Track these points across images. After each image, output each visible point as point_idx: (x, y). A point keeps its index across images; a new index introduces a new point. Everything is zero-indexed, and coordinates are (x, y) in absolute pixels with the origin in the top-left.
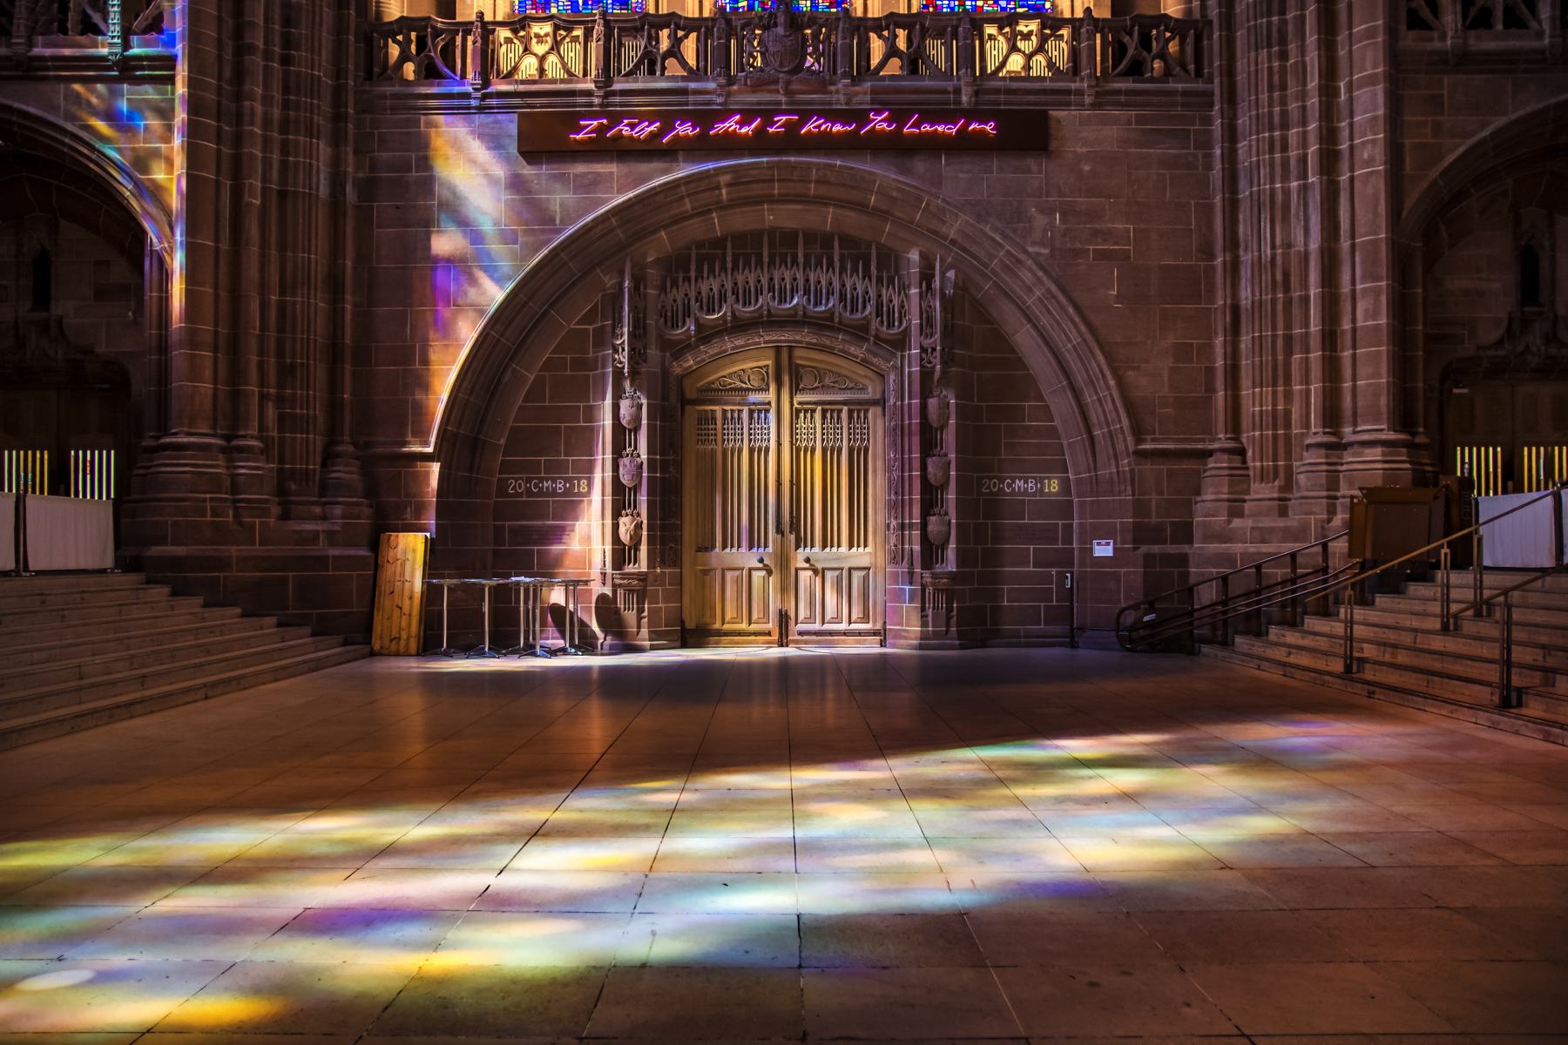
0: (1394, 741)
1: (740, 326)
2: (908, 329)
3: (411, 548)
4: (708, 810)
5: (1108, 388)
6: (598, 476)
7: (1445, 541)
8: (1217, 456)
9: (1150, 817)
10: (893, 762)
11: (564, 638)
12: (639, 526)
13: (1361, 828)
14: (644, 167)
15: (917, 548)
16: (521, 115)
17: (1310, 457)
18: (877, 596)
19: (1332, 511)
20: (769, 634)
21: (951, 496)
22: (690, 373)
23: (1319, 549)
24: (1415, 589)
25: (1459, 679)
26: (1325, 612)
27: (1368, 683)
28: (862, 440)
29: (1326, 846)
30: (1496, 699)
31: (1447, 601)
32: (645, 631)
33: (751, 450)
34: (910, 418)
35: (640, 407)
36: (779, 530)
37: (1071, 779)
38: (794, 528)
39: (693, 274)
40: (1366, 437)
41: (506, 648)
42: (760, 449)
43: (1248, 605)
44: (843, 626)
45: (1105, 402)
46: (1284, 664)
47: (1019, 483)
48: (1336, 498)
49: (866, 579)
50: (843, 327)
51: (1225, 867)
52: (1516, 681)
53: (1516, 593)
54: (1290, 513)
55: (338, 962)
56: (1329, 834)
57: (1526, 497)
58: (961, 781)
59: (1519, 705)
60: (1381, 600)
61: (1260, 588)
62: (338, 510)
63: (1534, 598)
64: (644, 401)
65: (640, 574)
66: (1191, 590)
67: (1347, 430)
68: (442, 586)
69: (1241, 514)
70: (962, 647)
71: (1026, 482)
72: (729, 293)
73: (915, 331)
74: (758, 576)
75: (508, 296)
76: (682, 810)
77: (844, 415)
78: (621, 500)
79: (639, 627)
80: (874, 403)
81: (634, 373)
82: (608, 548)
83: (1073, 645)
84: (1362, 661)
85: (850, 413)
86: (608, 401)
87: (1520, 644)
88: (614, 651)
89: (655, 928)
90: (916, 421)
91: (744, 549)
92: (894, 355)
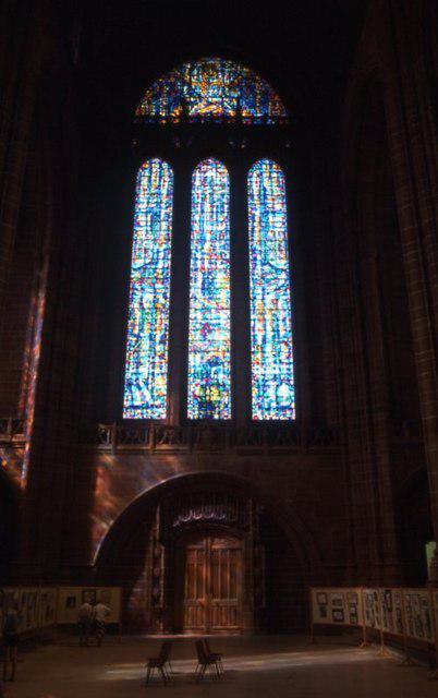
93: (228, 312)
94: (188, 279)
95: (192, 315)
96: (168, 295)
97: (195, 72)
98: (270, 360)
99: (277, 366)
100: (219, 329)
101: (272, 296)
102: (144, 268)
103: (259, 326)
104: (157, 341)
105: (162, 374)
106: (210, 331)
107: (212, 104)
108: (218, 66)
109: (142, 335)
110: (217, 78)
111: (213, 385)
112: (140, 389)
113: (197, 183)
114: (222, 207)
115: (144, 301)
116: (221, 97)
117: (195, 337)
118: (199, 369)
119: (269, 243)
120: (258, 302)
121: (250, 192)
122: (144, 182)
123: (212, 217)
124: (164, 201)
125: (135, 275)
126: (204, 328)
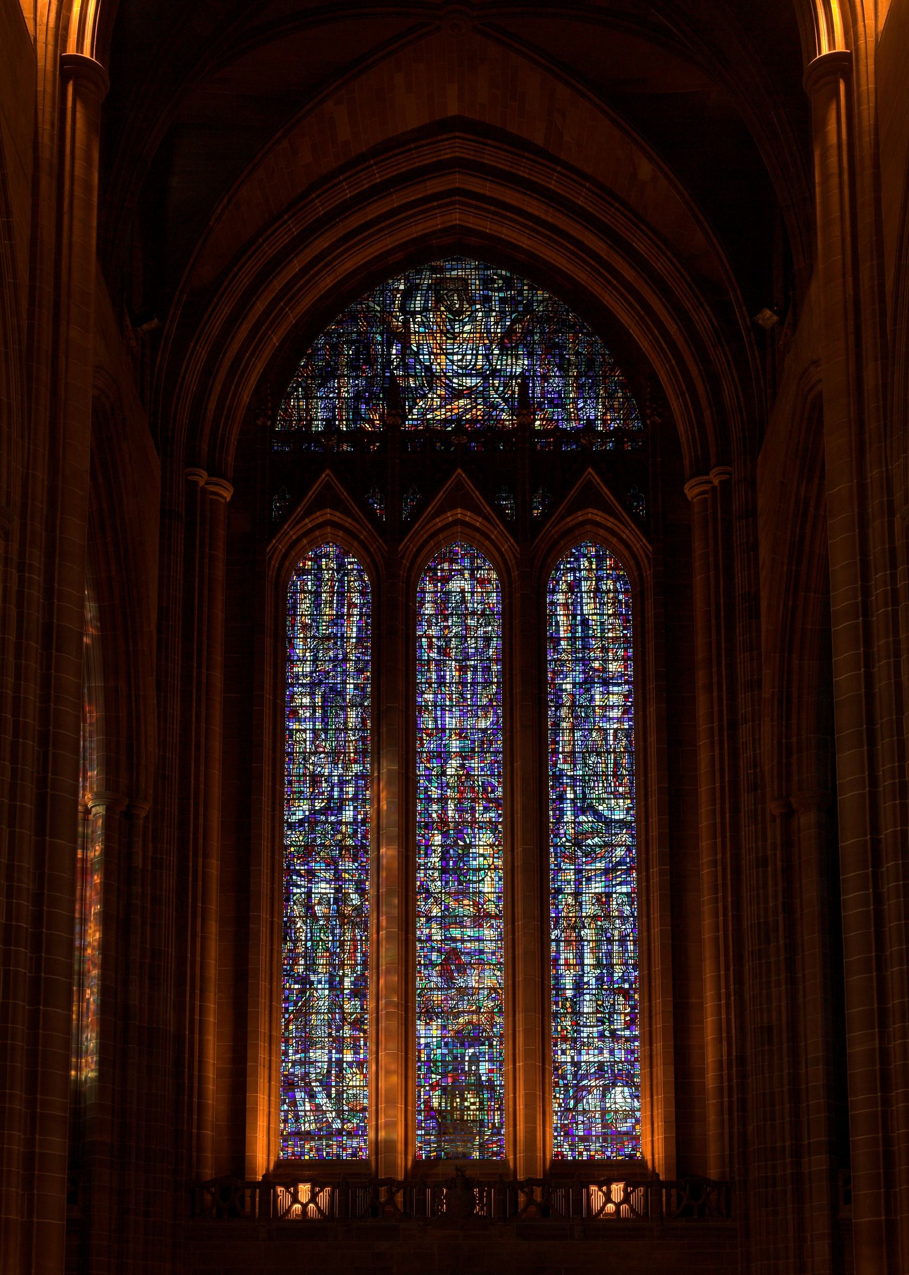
93: (500, 923)
95: (422, 932)
97: (418, 304)
99: (608, 1043)
100: (481, 963)
101: (597, 887)
102: (311, 821)
103: (567, 955)
106: (462, 969)
107: (457, 394)
108: (475, 284)
110: (473, 319)
111: (468, 1087)
112: (312, 1096)
114: (486, 670)
115: (315, 899)
116: (480, 374)
119: (593, 759)
122: (305, 606)
123: (462, 695)
125: (294, 838)
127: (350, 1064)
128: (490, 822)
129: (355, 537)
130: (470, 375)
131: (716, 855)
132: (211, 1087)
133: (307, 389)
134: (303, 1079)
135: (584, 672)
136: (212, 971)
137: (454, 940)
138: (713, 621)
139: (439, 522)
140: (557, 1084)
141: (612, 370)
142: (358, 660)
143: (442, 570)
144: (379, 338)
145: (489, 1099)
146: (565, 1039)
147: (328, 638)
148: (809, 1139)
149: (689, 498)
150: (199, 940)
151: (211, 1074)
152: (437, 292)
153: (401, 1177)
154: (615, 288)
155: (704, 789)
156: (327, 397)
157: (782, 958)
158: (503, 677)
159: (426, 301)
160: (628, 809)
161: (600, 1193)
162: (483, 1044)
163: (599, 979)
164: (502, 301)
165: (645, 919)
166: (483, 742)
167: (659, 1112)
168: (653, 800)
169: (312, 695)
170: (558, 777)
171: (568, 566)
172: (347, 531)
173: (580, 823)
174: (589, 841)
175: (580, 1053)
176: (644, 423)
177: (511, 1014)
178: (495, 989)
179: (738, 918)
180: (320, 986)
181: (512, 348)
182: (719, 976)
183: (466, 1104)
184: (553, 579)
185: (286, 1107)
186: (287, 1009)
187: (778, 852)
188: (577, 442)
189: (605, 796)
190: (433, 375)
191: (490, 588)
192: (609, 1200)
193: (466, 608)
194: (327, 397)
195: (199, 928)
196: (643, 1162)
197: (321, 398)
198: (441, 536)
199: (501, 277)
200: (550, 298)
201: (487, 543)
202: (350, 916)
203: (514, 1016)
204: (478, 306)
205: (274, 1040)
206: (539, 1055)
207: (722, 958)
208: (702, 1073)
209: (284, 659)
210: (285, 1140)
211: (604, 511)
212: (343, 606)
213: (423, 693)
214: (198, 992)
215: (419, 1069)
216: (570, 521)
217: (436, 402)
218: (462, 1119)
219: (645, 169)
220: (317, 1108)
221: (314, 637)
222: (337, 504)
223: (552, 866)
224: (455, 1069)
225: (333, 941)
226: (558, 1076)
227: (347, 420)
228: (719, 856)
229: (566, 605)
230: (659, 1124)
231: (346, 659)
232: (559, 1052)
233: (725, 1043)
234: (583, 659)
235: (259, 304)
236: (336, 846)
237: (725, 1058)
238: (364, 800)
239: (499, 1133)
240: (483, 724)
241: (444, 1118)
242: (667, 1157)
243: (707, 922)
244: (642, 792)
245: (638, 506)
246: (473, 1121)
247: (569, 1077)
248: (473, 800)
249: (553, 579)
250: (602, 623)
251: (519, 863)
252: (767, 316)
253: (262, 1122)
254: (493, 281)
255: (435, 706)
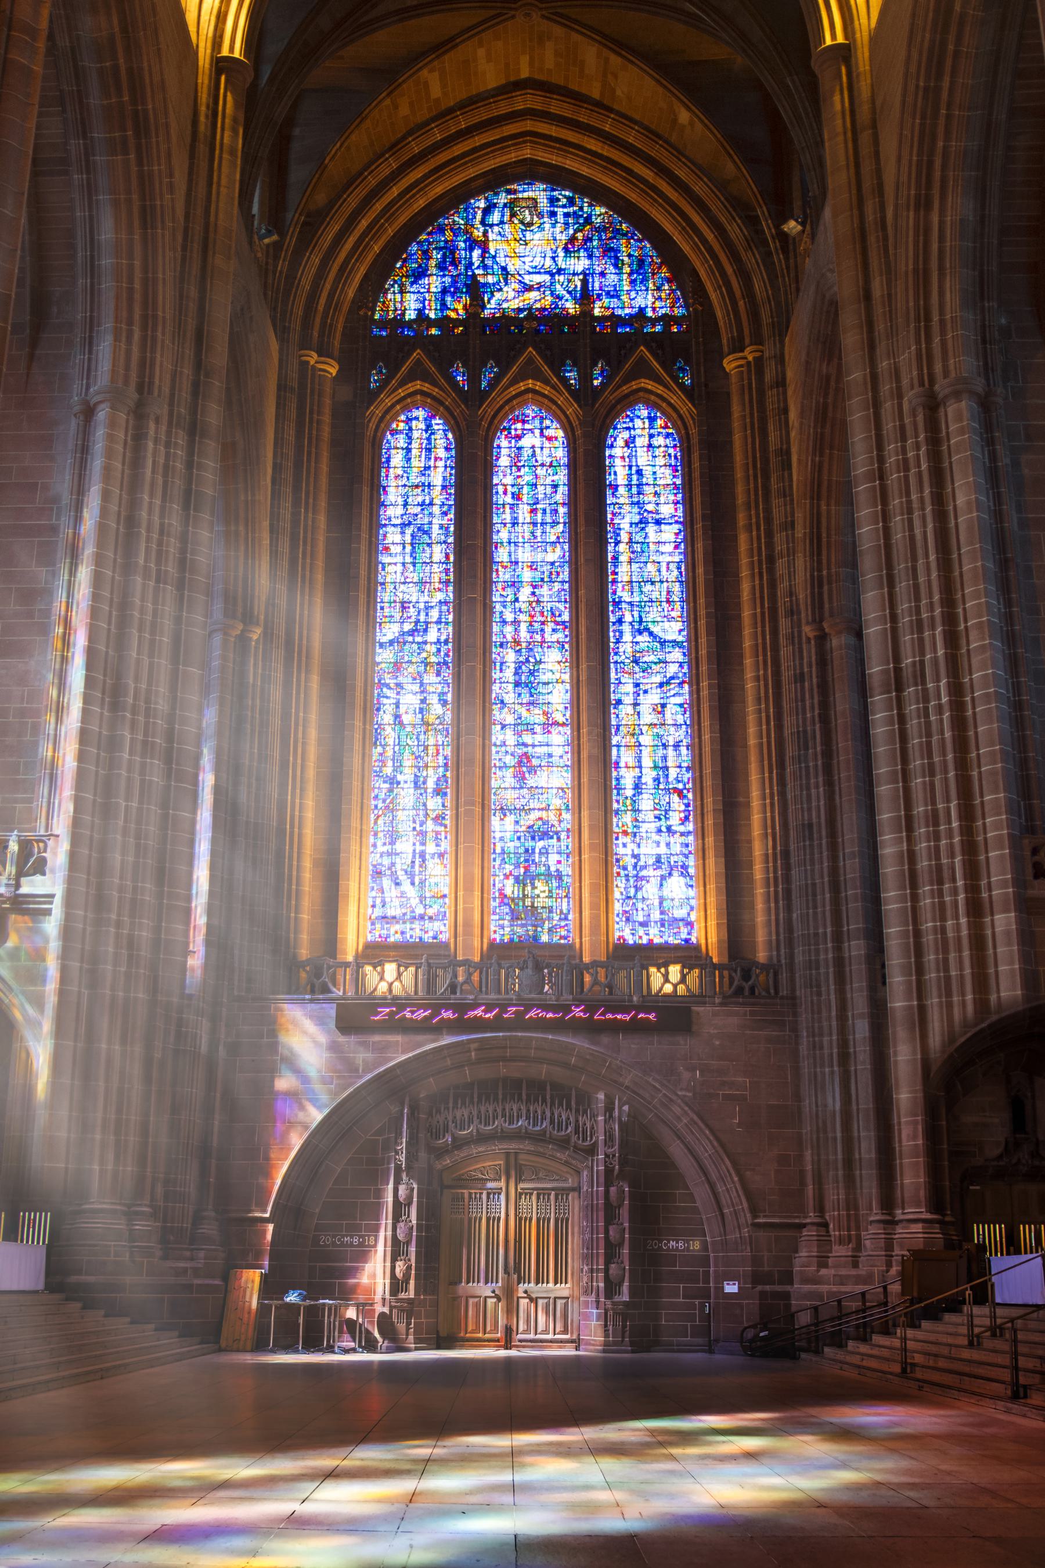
0: (939, 1421)
1: (482, 1138)
2: (596, 1142)
3: (252, 1279)
4: (452, 1461)
5: (733, 1182)
6: (382, 1234)
7: (968, 1286)
8: (809, 1227)
9: (766, 1470)
10: (584, 1429)
11: (354, 1341)
12: (409, 1268)
13: (917, 1480)
14: (420, 1038)
15: (602, 1285)
16: (338, 1004)
17: (872, 1230)
18: (573, 1315)
19: (889, 1265)
20: (498, 1341)
21: (626, 1251)
22: (447, 1168)
23: (881, 1290)
24: (948, 1317)
25: (982, 1378)
26: (886, 1331)
27: (918, 1380)
28: (565, 1214)
29: (892, 1493)
30: (1009, 1392)
31: (971, 1325)
32: (411, 1338)
33: (488, 1219)
34: (597, 1200)
35: (412, 1189)
36: (506, 1271)
37: (710, 1443)
38: (517, 1271)
39: (451, 1105)
40: (911, 1217)
41: (314, 1347)
42: (494, 1218)
43: (832, 1326)
44: (550, 1336)
45: (731, 1193)
46: (859, 1367)
47: (672, 1244)
48: (892, 1256)
49: (566, 1305)
50: (552, 1140)
51: (821, 1505)
52: (1022, 1380)
53: (1019, 1321)
54: (860, 1266)
55: (184, 1563)
56: (895, 1484)
57: (1023, 1257)
58: (632, 1444)
59: (1025, 1397)
60: (925, 1324)
61: (841, 1314)
62: (202, 1254)
63: (1032, 1325)
64: (415, 1186)
65: (409, 1299)
66: (793, 1315)
67: (899, 1212)
68: (271, 1306)
69: (826, 1266)
70: (633, 1352)
71: (677, 1242)
72: (475, 1118)
73: (601, 1144)
74: (491, 1302)
75: (325, 1117)
76: (434, 1460)
77: (552, 1197)
78: (397, 1250)
79: (407, 1334)
80: (573, 1189)
81: (409, 1167)
82: (388, 1281)
83: (711, 1351)
84: (913, 1365)
85: (557, 1196)
86: (391, 1186)
87: (1024, 1355)
88: (389, 1351)
89: (413, 1543)
90: (601, 1201)
91: (481, 1284)
92: (587, 1159)
93: (568, 730)
94: (487, 664)
95: (497, 735)
96: (449, 697)
97: (495, 217)
98: (649, 827)
99: (664, 838)
101: (654, 697)
103: (627, 757)
104: (430, 790)
105: (441, 855)
106: (533, 770)
107: (528, 288)
109: (400, 778)
113: (504, 461)
115: (402, 709)
117: (502, 781)
118: (511, 846)
119: (648, 587)
120: (626, 710)
121: (610, 479)
122: (397, 459)
124: (437, 501)
125: (385, 656)
126: (520, 762)
127: (433, 856)
128: (558, 642)
129: (441, 403)
130: (539, 273)
131: (758, 671)
132: (307, 875)
133: (402, 286)
134: (389, 869)
135: (639, 513)
136: (311, 773)
137: (525, 745)
138: (751, 472)
139: (513, 391)
140: (619, 874)
141: (659, 268)
142: (443, 504)
143: (516, 430)
144: (462, 245)
145: (558, 887)
146: (625, 833)
147: (417, 487)
148: (848, 925)
149: (727, 370)
150: (300, 745)
151: (307, 864)
152: (511, 209)
153: (477, 958)
154: (660, 205)
155: (746, 614)
156: (419, 292)
157: (820, 763)
158: (569, 517)
159: (503, 216)
160: (680, 631)
161: (659, 974)
162: (552, 838)
163: (657, 780)
164: (566, 215)
165: (696, 727)
166: (551, 573)
167: (712, 899)
168: (702, 623)
169: (403, 533)
170: (617, 604)
171: (625, 426)
172: (434, 398)
173: (637, 643)
174: (645, 659)
175: (639, 846)
176: (687, 310)
177: (577, 811)
178: (562, 789)
179: (779, 727)
180: (406, 786)
181: (574, 252)
182: (763, 778)
183: (537, 892)
184: (612, 436)
185: (374, 894)
186: (376, 807)
187: (814, 669)
188: (631, 326)
189: (659, 619)
190: (508, 273)
191: (556, 443)
192: (667, 980)
193: (536, 461)
194: (419, 292)
195: (300, 735)
196: (697, 948)
197: (414, 293)
198: (515, 402)
199: (565, 196)
200: (606, 213)
201: (554, 407)
202: (433, 724)
203: (580, 813)
204: (546, 220)
205: (364, 834)
206: (602, 849)
207: (766, 763)
208: (750, 865)
209: (377, 504)
210: (373, 924)
211: (654, 381)
212: (430, 459)
213: (498, 531)
214: (298, 791)
215: (494, 860)
216: (625, 389)
217: (511, 294)
218: (532, 906)
219: (684, 116)
220: (403, 894)
221: (405, 486)
222: (426, 377)
223: (612, 681)
224: (526, 861)
225: (418, 745)
226: (619, 867)
227: (436, 309)
228: (761, 672)
229: (623, 458)
230: (712, 911)
231: (431, 504)
232: (621, 845)
233: (770, 839)
234: (638, 503)
235: (363, 221)
236: (422, 662)
237: (770, 851)
238: (447, 623)
239: (566, 919)
240: (551, 557)
241: (517, 904)
242: (719, 941)
243: (752, 730)
244: (692, 616)
245: (683, 378)
246: (543, 907)
247: (630, 868)
248: (543, 623)
249: (612, 436)
250: (654, 473)
251: (583, 677)
252: (792, 226)
253: (352, 908)
254: (558, 200)
255: (510, 543)
